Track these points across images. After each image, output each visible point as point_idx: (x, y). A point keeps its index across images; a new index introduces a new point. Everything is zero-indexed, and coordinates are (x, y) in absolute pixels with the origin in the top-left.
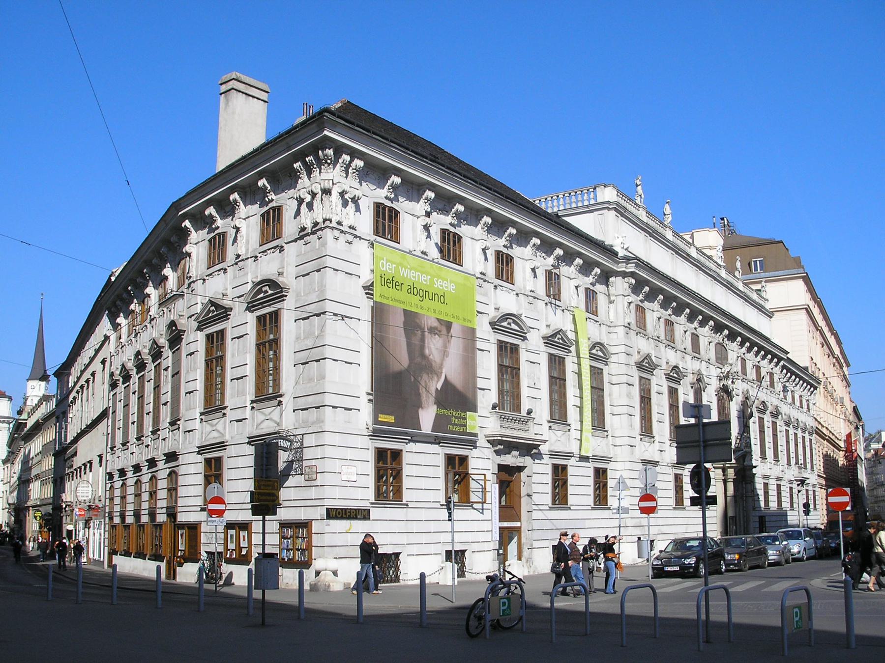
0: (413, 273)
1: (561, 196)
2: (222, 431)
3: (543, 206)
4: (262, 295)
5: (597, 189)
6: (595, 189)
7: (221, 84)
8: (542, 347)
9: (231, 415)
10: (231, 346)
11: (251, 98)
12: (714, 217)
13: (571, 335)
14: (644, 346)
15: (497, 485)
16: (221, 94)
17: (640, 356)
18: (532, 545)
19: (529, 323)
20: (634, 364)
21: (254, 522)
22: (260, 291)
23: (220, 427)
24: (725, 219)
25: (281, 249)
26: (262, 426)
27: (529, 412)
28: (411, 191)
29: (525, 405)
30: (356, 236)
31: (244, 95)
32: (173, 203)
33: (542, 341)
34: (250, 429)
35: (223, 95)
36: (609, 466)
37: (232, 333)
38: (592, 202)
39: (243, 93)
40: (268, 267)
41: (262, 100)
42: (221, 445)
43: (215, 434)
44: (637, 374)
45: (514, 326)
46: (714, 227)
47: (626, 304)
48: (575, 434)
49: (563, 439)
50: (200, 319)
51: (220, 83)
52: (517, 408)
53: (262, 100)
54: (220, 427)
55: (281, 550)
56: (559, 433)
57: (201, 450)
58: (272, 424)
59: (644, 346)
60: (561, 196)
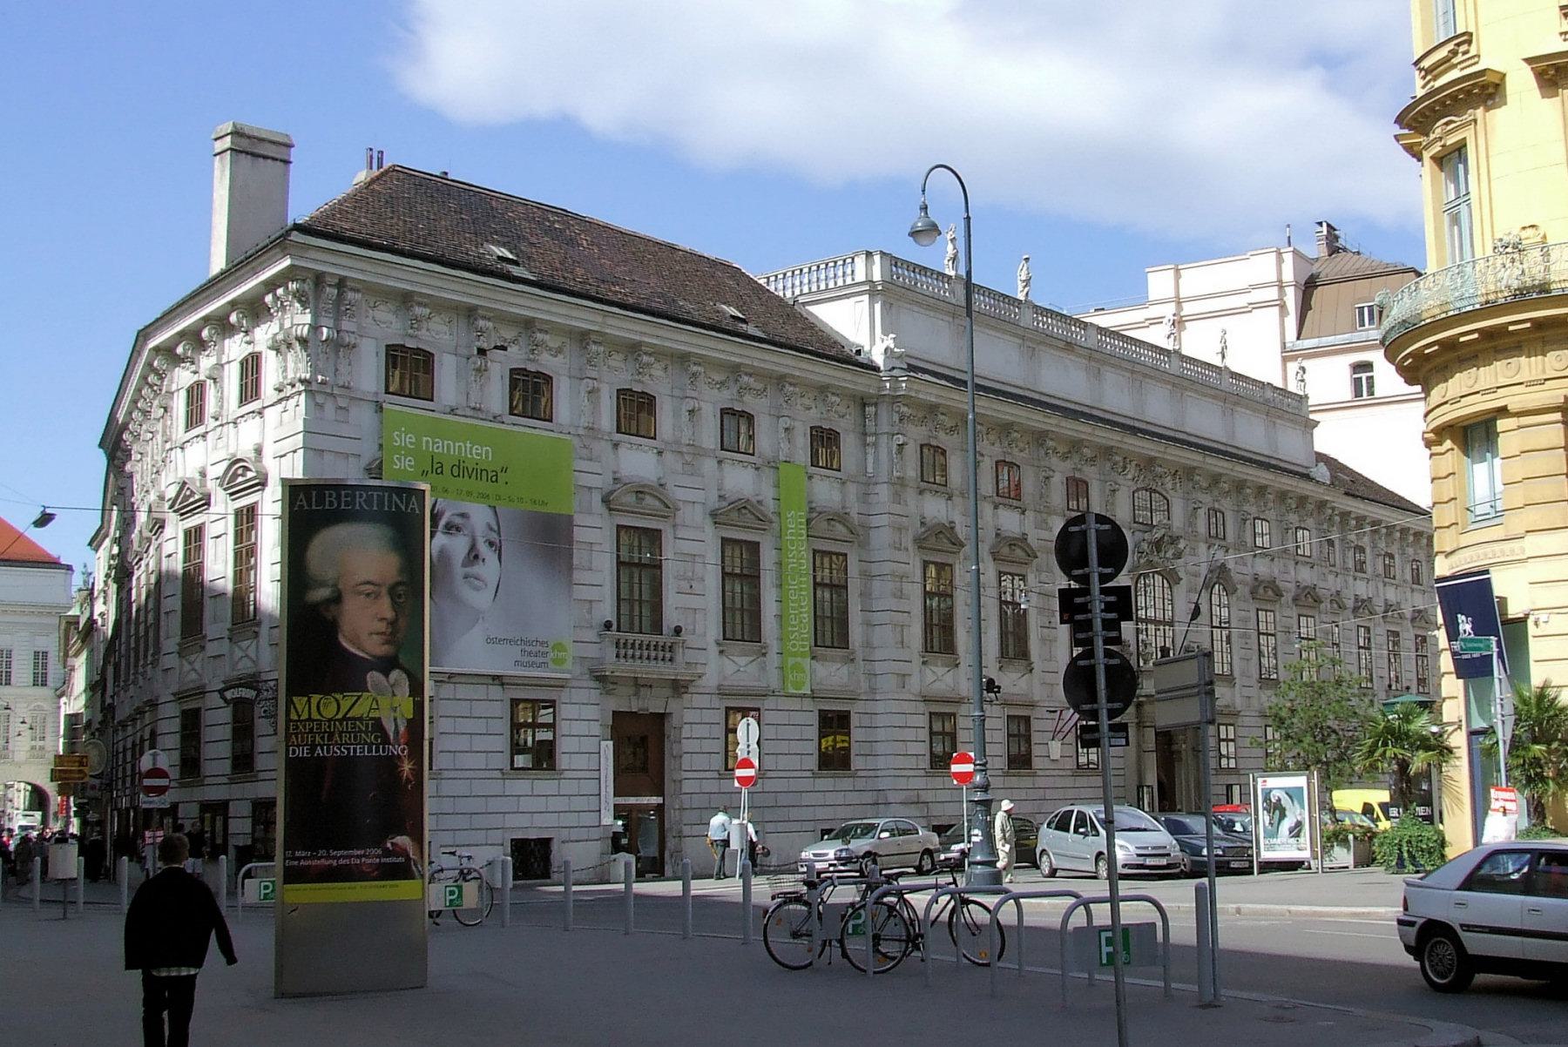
0: (410, 461)
1: (806, 270)
2: (200, 671)
3: (772, 288)
4: (240, 479)
5: (856, 259)
6: (853, 259)
7: (216, 139)
8: (709, 528)
9: (212, 649)
10: (209, 544)
11: (261, 160)
12: (1288, 226)
13: (770, 506)
14: (935, 509)
15: (611, 743)
16: (215, 155)
17: (923, 530)
18: (681, 832)
19: (680, 494)
20: (910, 546)
21: (231, 803)
22: (235, 475)
23: (197, 666)
24: (1325, 225)
25: (260, 413)
26: (240, 666)
27: (678, 631)
28: (455, 320)
29: (671, 618)
30: (352, 399)
31: (249, 157)
32: (139, 332)
33: (709, 521)
34: (225, 671)
35: (218, 157)
36: (855, 709)
37: (226, 526)
38: (849, 281)
39: (247, 153)
40: (243, 439)
41: (281, 161)
42: (201, 692)
43: (193, 676)
44: (917, 559)
45: (649, 500)
46: (1290, 245)
47: (895, 448)
48: (773, 659)
49: (753, 668)
50: (176, 507)
51: (213, 136)
52: (657, 627)
53: (281, 161)
54: (197, 666)
55: (254, 840)
56: (742, 661)
57: (180, 697)
58: (250, 664)
59: (935, 509)
60: (806, 270)
